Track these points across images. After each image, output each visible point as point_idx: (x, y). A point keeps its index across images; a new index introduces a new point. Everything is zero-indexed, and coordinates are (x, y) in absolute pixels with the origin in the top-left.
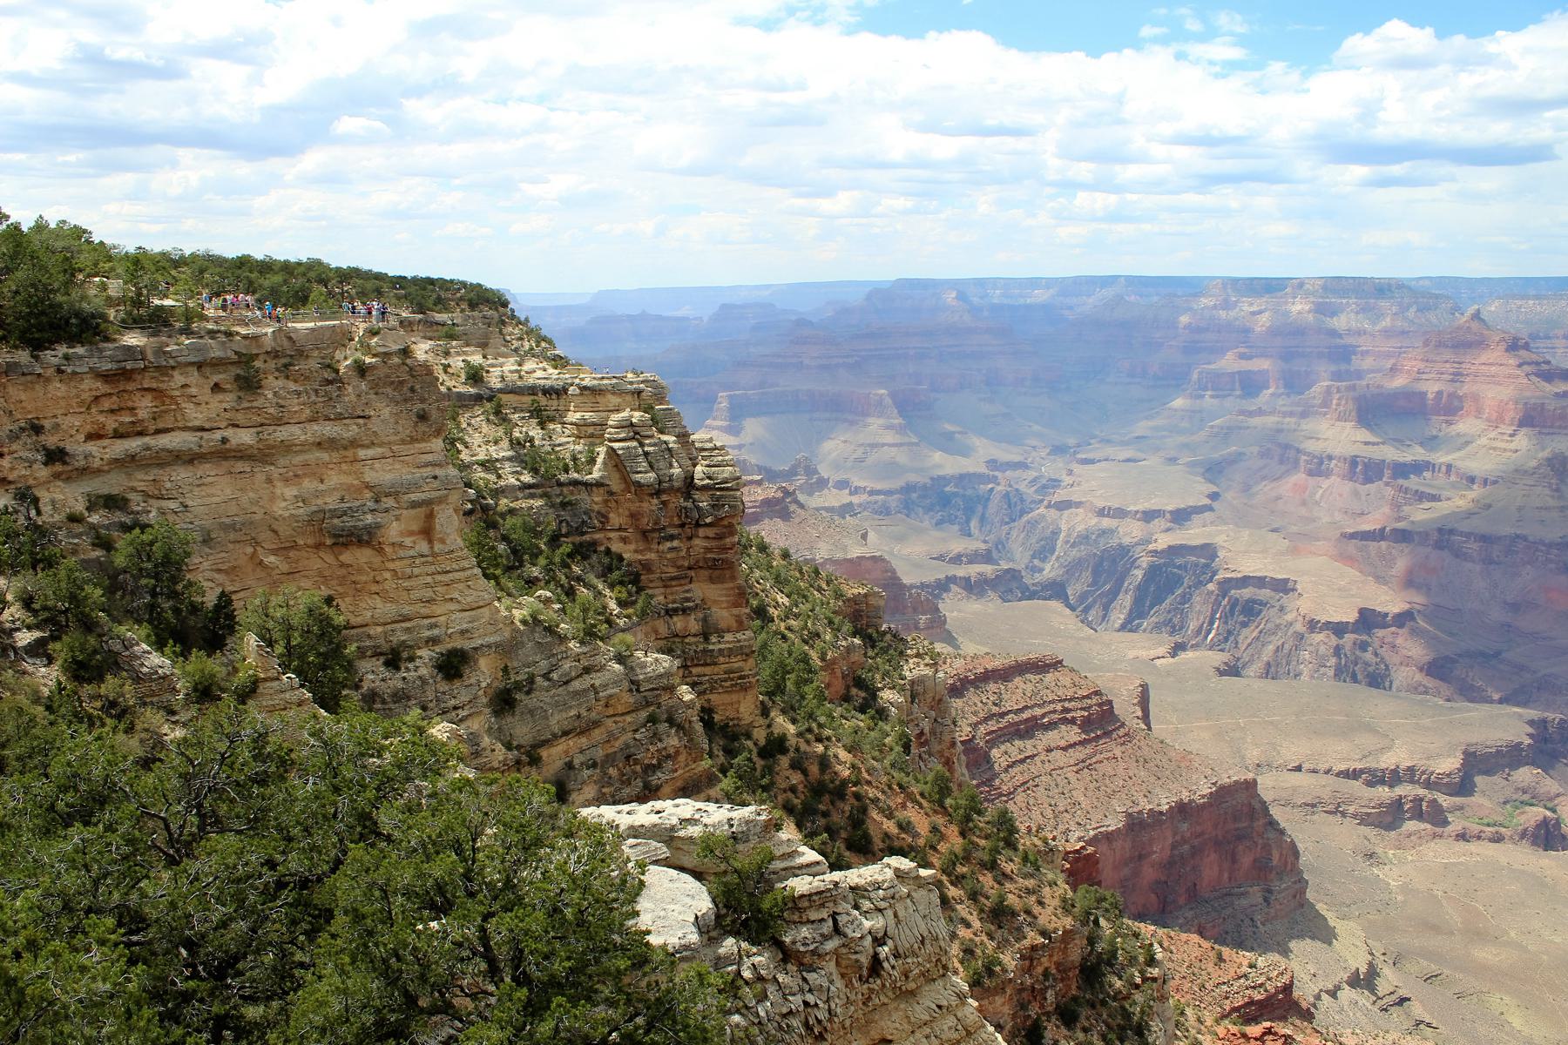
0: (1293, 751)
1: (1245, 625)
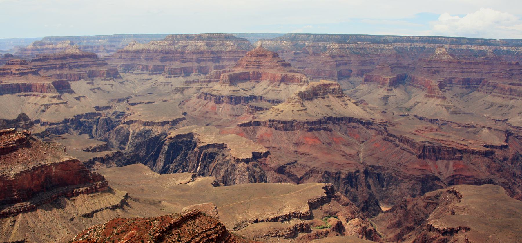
0: (253, 215)
1: (210, 162)
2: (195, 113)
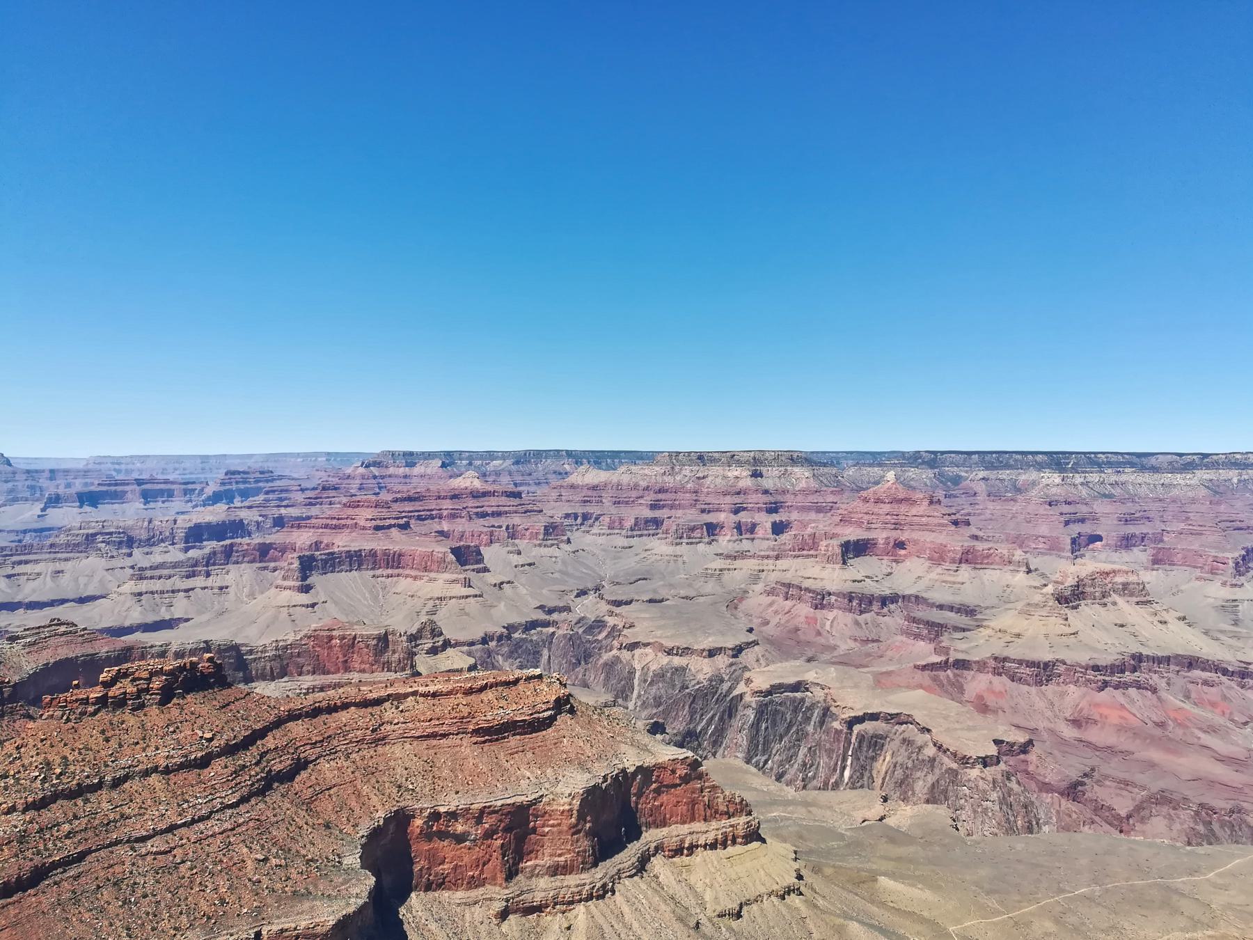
1: (874, 759)
2: (770, 630)
